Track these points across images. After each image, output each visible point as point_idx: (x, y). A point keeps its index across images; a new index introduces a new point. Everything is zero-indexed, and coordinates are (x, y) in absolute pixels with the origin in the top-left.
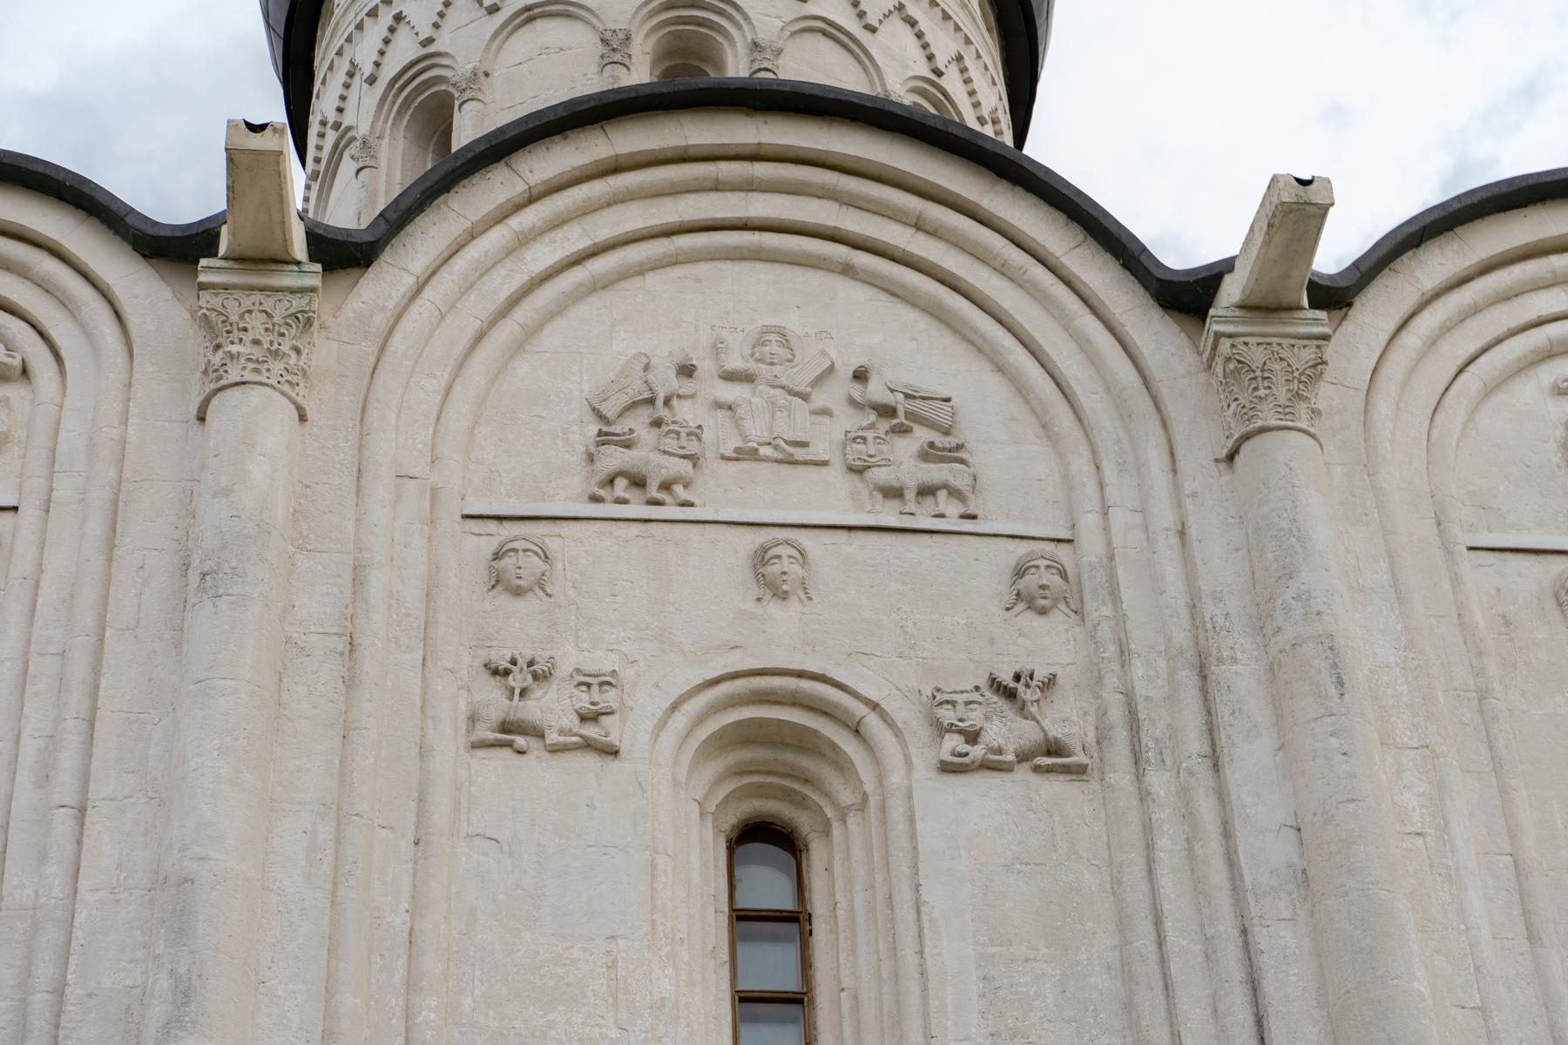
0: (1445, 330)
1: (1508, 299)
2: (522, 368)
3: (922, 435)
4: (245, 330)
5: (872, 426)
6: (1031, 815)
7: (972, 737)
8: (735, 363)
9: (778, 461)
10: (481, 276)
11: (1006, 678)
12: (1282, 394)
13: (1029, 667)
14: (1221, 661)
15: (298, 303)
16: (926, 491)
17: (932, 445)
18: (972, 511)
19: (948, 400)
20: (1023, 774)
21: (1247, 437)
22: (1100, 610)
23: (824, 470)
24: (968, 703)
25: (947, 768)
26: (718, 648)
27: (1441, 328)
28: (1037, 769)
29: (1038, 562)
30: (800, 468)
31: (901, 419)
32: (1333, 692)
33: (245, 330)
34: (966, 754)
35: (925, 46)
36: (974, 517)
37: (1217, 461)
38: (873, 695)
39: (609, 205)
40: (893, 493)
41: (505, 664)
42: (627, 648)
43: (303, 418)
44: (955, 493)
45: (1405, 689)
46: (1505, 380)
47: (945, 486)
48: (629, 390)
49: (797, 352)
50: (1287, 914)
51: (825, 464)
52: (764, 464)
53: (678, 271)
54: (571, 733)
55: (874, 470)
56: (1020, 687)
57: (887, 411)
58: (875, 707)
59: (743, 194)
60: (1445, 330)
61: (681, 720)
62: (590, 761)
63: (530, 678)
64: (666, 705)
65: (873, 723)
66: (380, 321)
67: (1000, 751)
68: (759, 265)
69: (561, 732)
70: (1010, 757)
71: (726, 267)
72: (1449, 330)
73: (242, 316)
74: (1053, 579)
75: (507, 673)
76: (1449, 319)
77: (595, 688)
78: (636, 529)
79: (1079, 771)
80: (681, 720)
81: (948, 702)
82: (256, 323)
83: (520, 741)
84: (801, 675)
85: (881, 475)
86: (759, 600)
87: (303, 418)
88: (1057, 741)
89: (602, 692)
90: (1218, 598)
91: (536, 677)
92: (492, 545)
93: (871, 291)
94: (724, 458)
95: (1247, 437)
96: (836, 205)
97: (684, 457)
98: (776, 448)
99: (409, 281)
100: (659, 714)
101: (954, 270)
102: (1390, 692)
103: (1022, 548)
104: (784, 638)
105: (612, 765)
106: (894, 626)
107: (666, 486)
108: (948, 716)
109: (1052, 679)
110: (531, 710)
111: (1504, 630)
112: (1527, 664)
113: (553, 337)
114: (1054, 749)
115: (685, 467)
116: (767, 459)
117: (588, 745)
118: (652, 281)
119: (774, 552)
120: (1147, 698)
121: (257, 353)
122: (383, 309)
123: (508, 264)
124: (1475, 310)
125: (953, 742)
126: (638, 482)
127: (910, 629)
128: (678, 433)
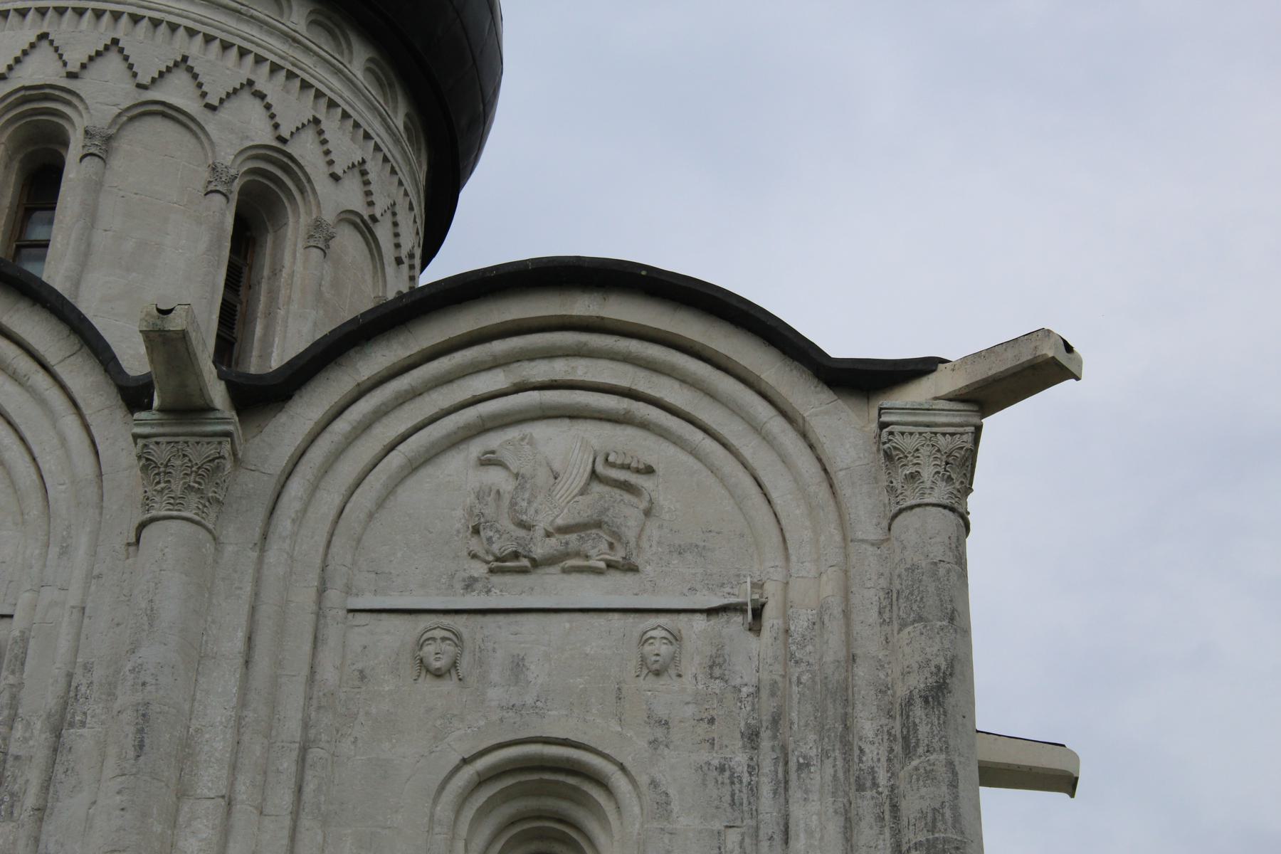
1: (451, 381)
12: (177, 487)
14: (71, 725)
21: (142, 526)
32: (132, 754)
35: (272, 116)
37: (129, 544)
72: (386, 413)
76: (383, 404)
90: (88, 668)
95: (142, 526)
102: (206, 748)
111: (357, 683)
112: (367, 713)
120: (17, 758)
124: (414, 394)
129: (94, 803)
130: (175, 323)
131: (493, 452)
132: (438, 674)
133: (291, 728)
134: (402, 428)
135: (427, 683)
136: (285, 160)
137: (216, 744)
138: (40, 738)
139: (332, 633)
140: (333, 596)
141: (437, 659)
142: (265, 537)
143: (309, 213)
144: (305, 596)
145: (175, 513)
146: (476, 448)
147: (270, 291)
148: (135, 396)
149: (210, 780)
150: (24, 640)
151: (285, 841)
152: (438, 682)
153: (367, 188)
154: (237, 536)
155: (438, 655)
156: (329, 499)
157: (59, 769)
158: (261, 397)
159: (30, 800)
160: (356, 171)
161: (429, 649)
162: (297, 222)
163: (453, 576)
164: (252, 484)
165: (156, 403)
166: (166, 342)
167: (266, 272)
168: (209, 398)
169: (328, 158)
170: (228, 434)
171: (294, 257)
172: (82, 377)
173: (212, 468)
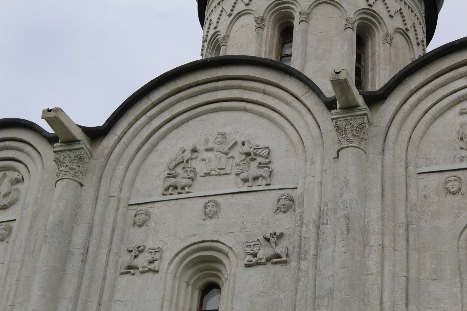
0: (420, 100)
1: (445, 85)
2: (151, 156)
3: (260, 160)
4: (64, 163)
5: (244, 160)
6: (269, 278)
7: (255, 255)
8: (210, 145)
9: (216, 175)
10: (139, 131)
11: (268, 236)
12: (350, 136)
13: (275, 231)
14: (323, 224)
15: (78, 152)
16: (256, 179)
17: (260, 163)
18: (268, 182)
19: (268, 148)
20: (269, 265)
21: (339, 151)
22: (298, 210)
23: (229, 176)
24: (254, 245)
25: (247, 266)
26: (190, 236)
27: (418, 100)
28: (272, 263)
29: (282, 197)
30: (222, 176)
31: (252, 156)
32: (345, 233)
33: (64, 163)
34: (252, 261)
36: (269, 185)
37: (335, 158)
38: (230, 244)
39: (177, 103)
40: (246, 180)
41: (131, 249)
42: (165, 240)
43: (82, 185)
44: (264, 178)
45: (377, 227)
46: (443, 113)
47: (261, 176)
48: (177, 160)
49: (228, 140)
50: (326, 304)
51: (229, 174)
52: (212, 177)
53: (199, 119)
54: (146, 267)
55: (241, 174)
56: (271, 238)
57: (248, 154)
58: (231, 248)
59: (216, 92)
60: (420, 100)
61: (177, 259)
62: (150, 275)
63: (137, 252)
64: (173, 255)
65: (230, 254)
66: (107, 151)
67: (261, 259)
68: (221, 113)
69: (143, 267)
70: (264, 261)
71: (212, 115)
72: (422, 100)
73: (64, 159)
74: (287, 202)
75: (132, 251)
77: (153, 253)
78: (174, 202)
79: (285, 262)
80: (177, 259)
81: (249, 245)
82: (67, 160)
83: (132, 271)
84: (212, 241)
85: (243, 176)
86: (204, 220)
87: (82, 185)
88: (278, 254)
89: (155, 254)
90: (326, 204)
91: (139, 252)
92: (134, 213)
93: (252, 115)
94: (202, 176)
95: (339, 151)
96: (242, 90)
97: (189, 178)
98: (216, 171)
99: (116, 138)
100: (171, 258)
101: (273, 106)
102: (372, 228)
103: (282, 192)
104: (209, 231)
105: (157, 275)
106: (239, 223)
107: (183, 188)
108: (248, 249)
109: (282, 235)
110: (136, 262)
112: (429, 210)
113: (161, 146)
114: (278, 256)
115: (190, 181)
116: (213, 175)
117: (150, 270)
118: (191, 123)
119: (208, 205)
120: (305, 238)
121: (67, 169)
122: (108, 148)
123: (147, 126)
125: (249, 258)
126: (175, 188)
127: (245, 223)
128: (188, 171)
129: (335, 251)
130: (342, 77)
131: (465, 109)
132: (454, 193)
133: (402, 218)
134: (429, 104)
135: (450, 197)
136: (372, 13)
137: (375, 226)
138: (312, 230)
139: (412, 182)
140: (411, 169)
141: (453, 188)
142: (383, 150)
143: (383, 31)
144: (401, 170)
145: (350, 145)
146: (458, 108)
147: (372, 62)
148: (330, 105)
149: (374, 240)
150: (302, 196)
151: (405, 259)
152: (454, 196)
153: (403, 19)
154: (373, 150)
155: (453, 186)
156: (405, 134)
157: (321, 240)
158: (375, 99)
159: (312, 252)
160: (399, 13)
161: (449, 184)
162: (379, 35)
163: (455, 157)
164: (376, 132)
165: (338, 106)
166: (339, 84)
167: (370, 55)
168: (357, 101)
169: (388, 10)
170: (365, 114)
171: (380, 48)
172: (311, 100)
173: (361, 127)
